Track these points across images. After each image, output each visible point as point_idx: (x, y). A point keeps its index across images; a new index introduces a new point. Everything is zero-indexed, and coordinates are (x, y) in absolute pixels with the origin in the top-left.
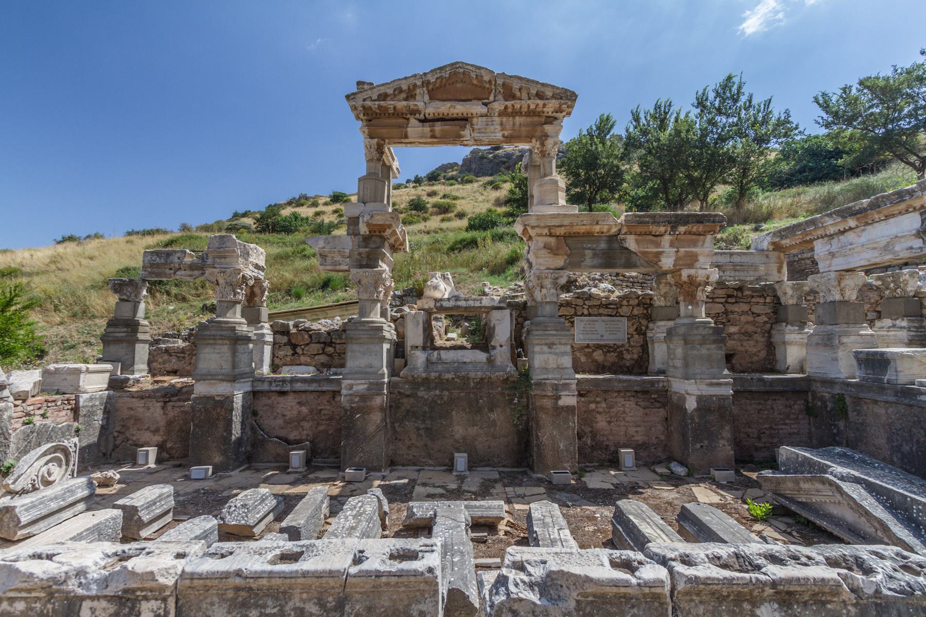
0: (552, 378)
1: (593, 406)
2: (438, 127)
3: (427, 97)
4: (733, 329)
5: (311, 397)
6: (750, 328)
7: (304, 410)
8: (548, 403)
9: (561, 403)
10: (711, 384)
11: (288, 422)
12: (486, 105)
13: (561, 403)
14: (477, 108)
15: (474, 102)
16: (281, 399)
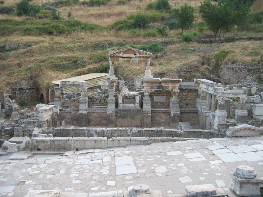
0: (147, 110)
1: (156, 115)
2: (125, 59)
3: (123, 53)
4: (188, 99)
5: (99, 113)
6: (192, 98)
7: (98, 115)
8: (145, 115)
9: (148, 115)
10: (176, 112)
11: (95, 118)
12: (135, 55)
13: (148, 115)
14: (133, 56)
15: (133, 54)
16: (93, 113)
